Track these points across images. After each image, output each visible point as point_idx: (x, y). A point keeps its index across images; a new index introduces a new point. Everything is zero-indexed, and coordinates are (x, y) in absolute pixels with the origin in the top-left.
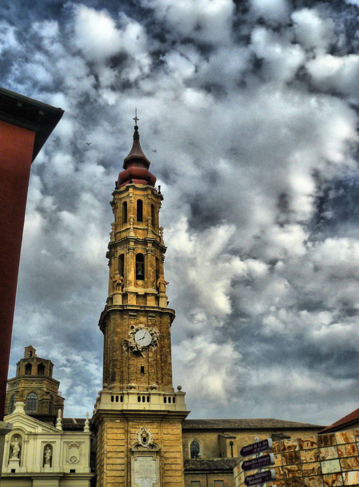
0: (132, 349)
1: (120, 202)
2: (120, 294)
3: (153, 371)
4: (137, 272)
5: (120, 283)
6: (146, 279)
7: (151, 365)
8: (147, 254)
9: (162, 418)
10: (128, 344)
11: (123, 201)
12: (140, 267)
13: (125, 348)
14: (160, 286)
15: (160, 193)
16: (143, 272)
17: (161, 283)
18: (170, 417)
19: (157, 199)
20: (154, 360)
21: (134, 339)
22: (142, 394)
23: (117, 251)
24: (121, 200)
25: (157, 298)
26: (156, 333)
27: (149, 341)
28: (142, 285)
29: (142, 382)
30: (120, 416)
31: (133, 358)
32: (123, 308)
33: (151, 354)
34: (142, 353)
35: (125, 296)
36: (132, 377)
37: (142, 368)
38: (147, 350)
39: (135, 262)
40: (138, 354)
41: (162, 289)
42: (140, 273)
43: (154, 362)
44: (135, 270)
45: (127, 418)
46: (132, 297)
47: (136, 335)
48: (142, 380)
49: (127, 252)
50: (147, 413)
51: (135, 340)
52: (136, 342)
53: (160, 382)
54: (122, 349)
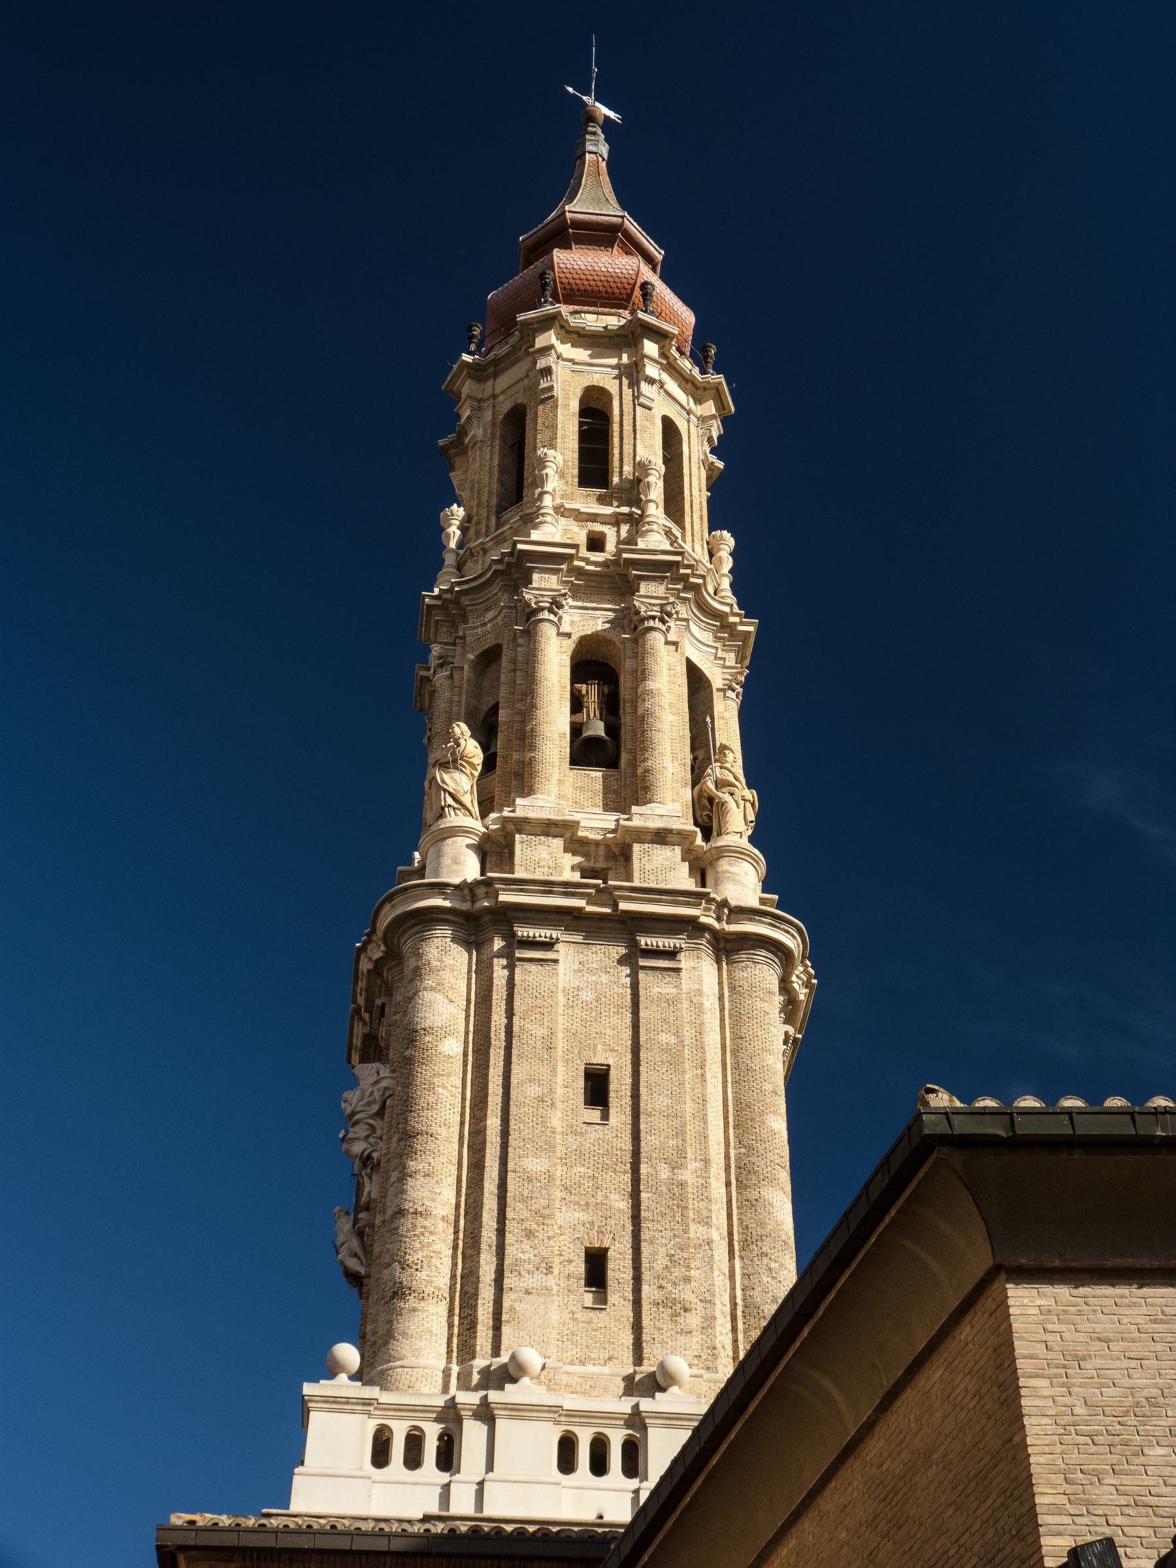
8: (635, 641)
11: (505, 406)
22: (586, 1416)
23: (464, 637)
25: (701, 869)
35: (495, 850)
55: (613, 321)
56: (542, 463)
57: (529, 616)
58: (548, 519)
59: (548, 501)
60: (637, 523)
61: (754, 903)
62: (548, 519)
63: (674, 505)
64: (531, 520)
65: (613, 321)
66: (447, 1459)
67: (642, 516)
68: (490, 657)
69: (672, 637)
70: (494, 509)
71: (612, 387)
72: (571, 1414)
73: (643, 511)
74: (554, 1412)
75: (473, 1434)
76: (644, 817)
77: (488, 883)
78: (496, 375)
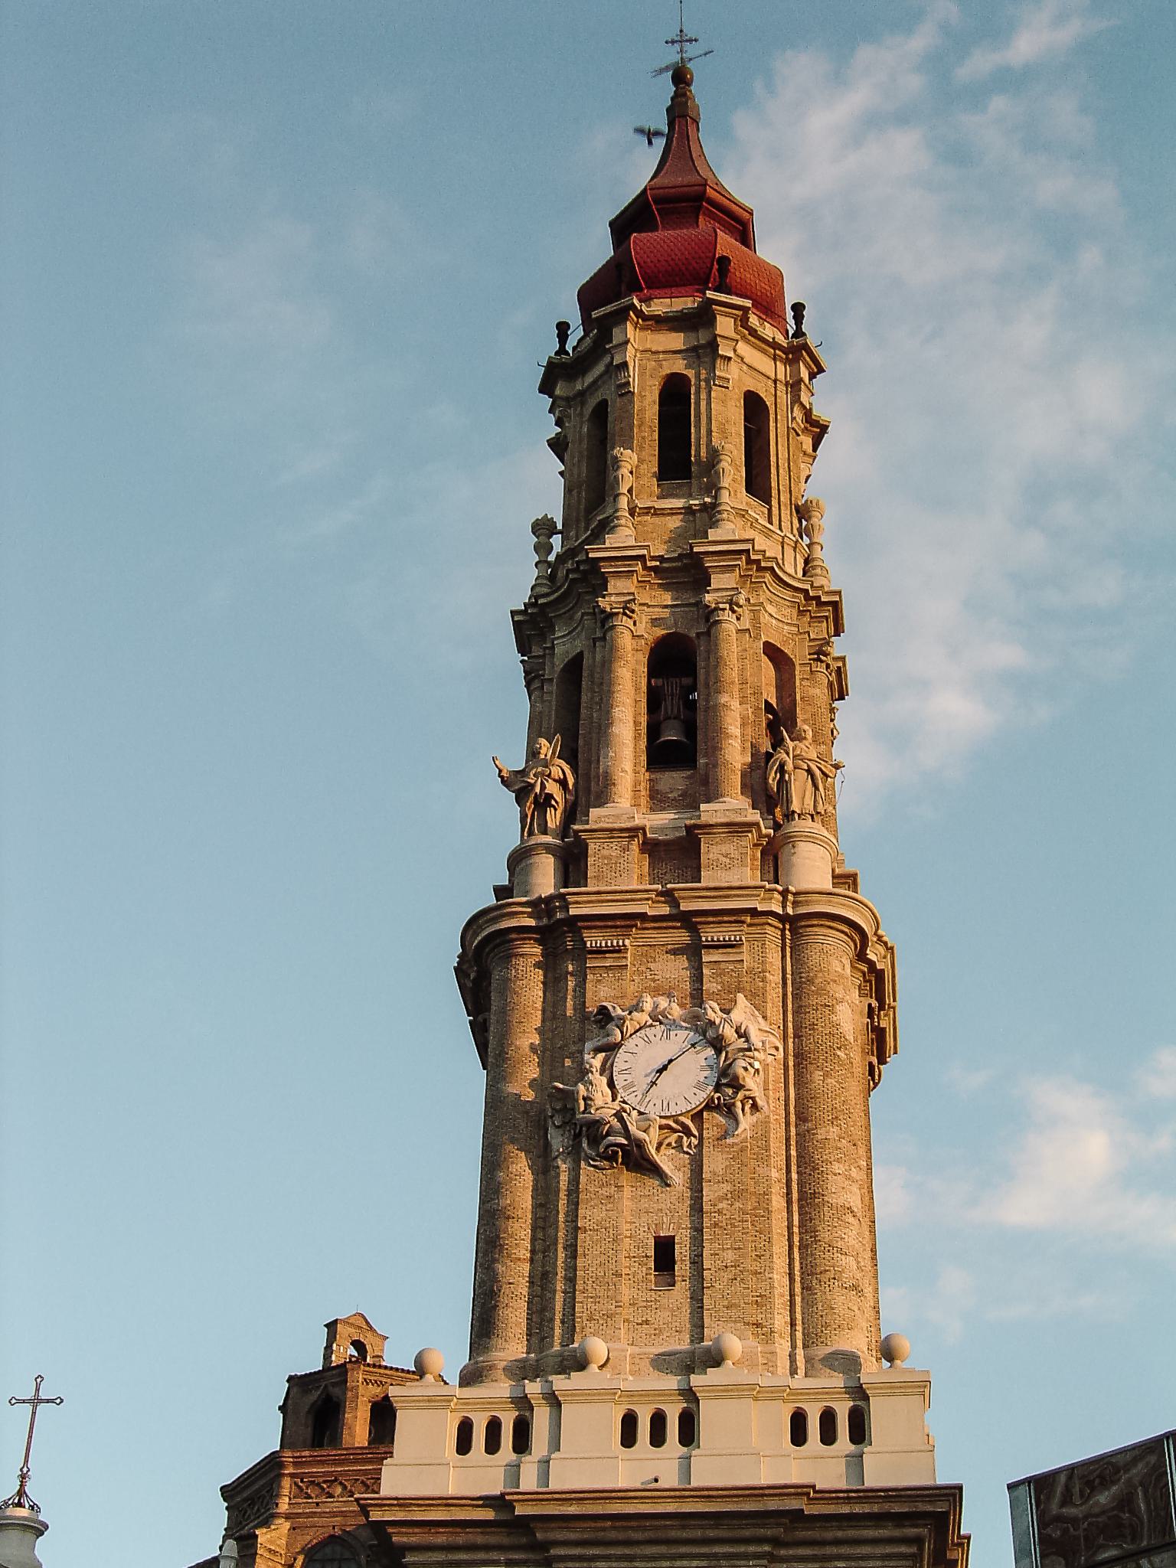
0: (595, 1141)
1: (581, 415)
2: (548, 848)
3: (730, 1256)
4: (653, 731)
5: (550, 796)
6: (702, 761)
7: (716, 1225)
8: (708, 633)
9: (776, 1542)
10: (573, 1111)
11: (592, 402)
12: (671, 705)
13: (558, 1141)
14: (781, 782)
15: (799, 333)
16: (690, 729)
17: (789, 767)
18: (829, 1535)
19: (780, 366)
20: (737, 1195)
21: (611, 1084)
22: (645, 1395)
23: (553, 648)
24: (583, 404)
26: (742, 1034)
27: (699, 1086)
28: (684, 794)
29: (658, 1332)
30: (492, 1540)
31: (604, 1192)
32: (550, 913)
33: (714, 1162)
34: (665, 1160)
35: (573, 862)
36: (596, 1300)
37: (664, 1252)
38: (695, 1141)
39: (644, 681)
40: (637, 1160)
41: (800, 795)
42: (671, 736)
43: (737, 1205)
44: (644, 720)
45: (545, 1546)
46: (609, 857)
47: (621, 1060)
48: (661, 1317)
49: (599, 634)
50: (671, 1508)
51: (619, 1082)
52: (622, 1094)
53: (781, 1321)
54: (547, 1145)
55: (685, 303)
56: (616, 462)
57: (605, 620)
58: (623, 522)
59: (623, 502)
60: (710, 514)
61: (827, 885)
62: (623, 522)
63: (758, 483)
64: (606, 526)
65: (685, 303)
66: (522, 1444)
67: (714, 505)
68: (575, 666)
69: (746, 623)
70: (582, 513)
71: (690, 373)
72: (630, 1394)
73: (716, 497)
74: (610, 1394)
75: (541, 1418)
76: (710, 812)
77: (562, 897)
78: (584, 372)
